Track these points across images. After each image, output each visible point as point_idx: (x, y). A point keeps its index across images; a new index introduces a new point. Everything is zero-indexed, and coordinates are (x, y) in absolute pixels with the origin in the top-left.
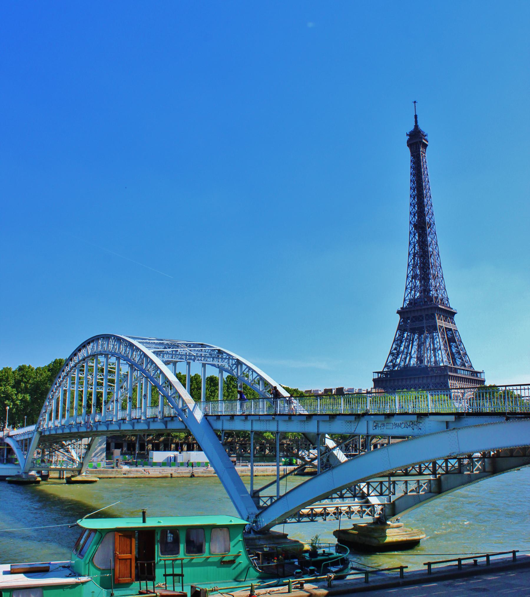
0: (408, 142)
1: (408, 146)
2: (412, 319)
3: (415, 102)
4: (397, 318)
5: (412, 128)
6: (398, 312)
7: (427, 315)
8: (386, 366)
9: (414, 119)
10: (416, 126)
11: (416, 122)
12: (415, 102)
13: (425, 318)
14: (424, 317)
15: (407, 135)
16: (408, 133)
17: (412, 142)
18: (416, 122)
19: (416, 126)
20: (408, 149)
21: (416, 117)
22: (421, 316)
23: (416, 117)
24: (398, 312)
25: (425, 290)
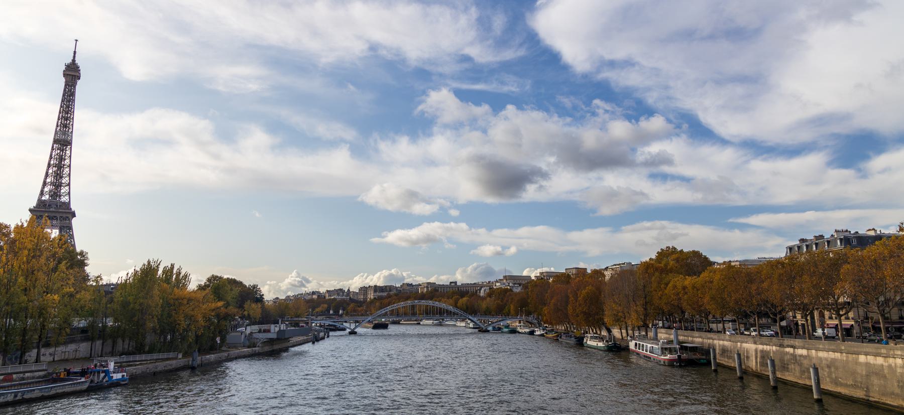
0: (64, 71)
5: (69, 61)
6: (30, 210)
7: (62, 217)
9: (73, 55)
10: (74, 60)
11: (74, 57)
12: (76, 40)
13: (60, 219)
14: (59, 219)
15: (66, 65)
16: (67, 64)
17: (68, 73)
18: (74, 57)
19: (74, 60)
20: (63, 80)
21: (75, 52)
22: (55, 217)
23: (75, 52)
24: (30, 210)
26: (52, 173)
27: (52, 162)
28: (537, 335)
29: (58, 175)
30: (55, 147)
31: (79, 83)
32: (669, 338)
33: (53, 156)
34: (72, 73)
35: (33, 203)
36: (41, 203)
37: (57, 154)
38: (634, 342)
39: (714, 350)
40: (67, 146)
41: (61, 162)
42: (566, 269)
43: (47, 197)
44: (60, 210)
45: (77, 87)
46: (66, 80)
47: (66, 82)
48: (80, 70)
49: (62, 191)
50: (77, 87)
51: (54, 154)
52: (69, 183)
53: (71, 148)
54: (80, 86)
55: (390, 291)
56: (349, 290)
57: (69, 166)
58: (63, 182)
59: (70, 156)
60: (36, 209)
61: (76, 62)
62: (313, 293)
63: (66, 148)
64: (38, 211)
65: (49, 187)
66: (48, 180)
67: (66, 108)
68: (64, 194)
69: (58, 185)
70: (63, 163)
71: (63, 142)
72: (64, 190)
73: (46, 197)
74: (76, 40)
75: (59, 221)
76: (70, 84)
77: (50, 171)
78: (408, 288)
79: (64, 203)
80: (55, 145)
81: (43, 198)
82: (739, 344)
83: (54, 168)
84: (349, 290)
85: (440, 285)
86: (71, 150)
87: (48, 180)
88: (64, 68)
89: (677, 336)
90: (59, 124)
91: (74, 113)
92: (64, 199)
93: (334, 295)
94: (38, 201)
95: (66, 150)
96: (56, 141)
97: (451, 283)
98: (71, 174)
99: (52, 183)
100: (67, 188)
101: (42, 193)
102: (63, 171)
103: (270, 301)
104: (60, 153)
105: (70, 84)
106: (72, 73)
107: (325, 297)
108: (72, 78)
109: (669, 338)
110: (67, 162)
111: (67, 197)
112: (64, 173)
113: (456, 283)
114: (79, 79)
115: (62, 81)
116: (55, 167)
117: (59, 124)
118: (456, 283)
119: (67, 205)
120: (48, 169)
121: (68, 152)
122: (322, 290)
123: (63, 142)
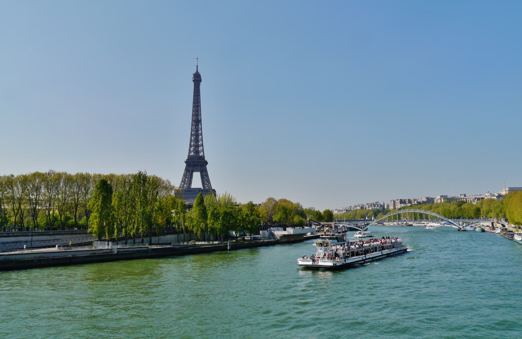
2: (193, 166)
3: (197, 59)
4: (185, 164)
5: (195, 72)
8: (181, 187)
9: (196, 67)
10: (197, 71)
15: (193, 75)
17: (195, 79)
19: (197, 71)
20: (193, 83)
21: (197, 66)
22: (197, 165)
23: (197, 66)
25: (197, 152)
29: (197, 140)
31: (201, 84)
34: (197, 79)
35: (186, 158)
40: (199, 122)
41: (197, 132)
44: (200, 161)
45: (200, 86)
46: (194, 83)
47: (194, 84)
48: (201, 76)
49: (200, 149)
50: (201, 87)
51: (193, 128)
57: (201, 134)
60: (188, 161)
61: (199, 72)
64: (189, 162)
65: (193, 147)
69: (197, 146)
70: (198, 133)
71: (197, 121)
72: (200, 149)
73: (192, 154)
74: (197, 59)
75: (199, 167)
76: (197, 85)
77: (192, 138)
79: (201, 156)
81: (191, 154)
87: (192, 144)
88: (192, 76)
90: (194, 110)
92: (201, 154)
95: (199, 125)
96: (193, 121)
99: (194, 146)
100: (201, 147)
105: (197, 85)
106: (197, 79)
108: (197, 82)
111: (202, 153)
112: (199, 139)
117: (194, 110)
119: (203, 158)
120: (191, 138)
121: (200, 126)
123: (197, 121)
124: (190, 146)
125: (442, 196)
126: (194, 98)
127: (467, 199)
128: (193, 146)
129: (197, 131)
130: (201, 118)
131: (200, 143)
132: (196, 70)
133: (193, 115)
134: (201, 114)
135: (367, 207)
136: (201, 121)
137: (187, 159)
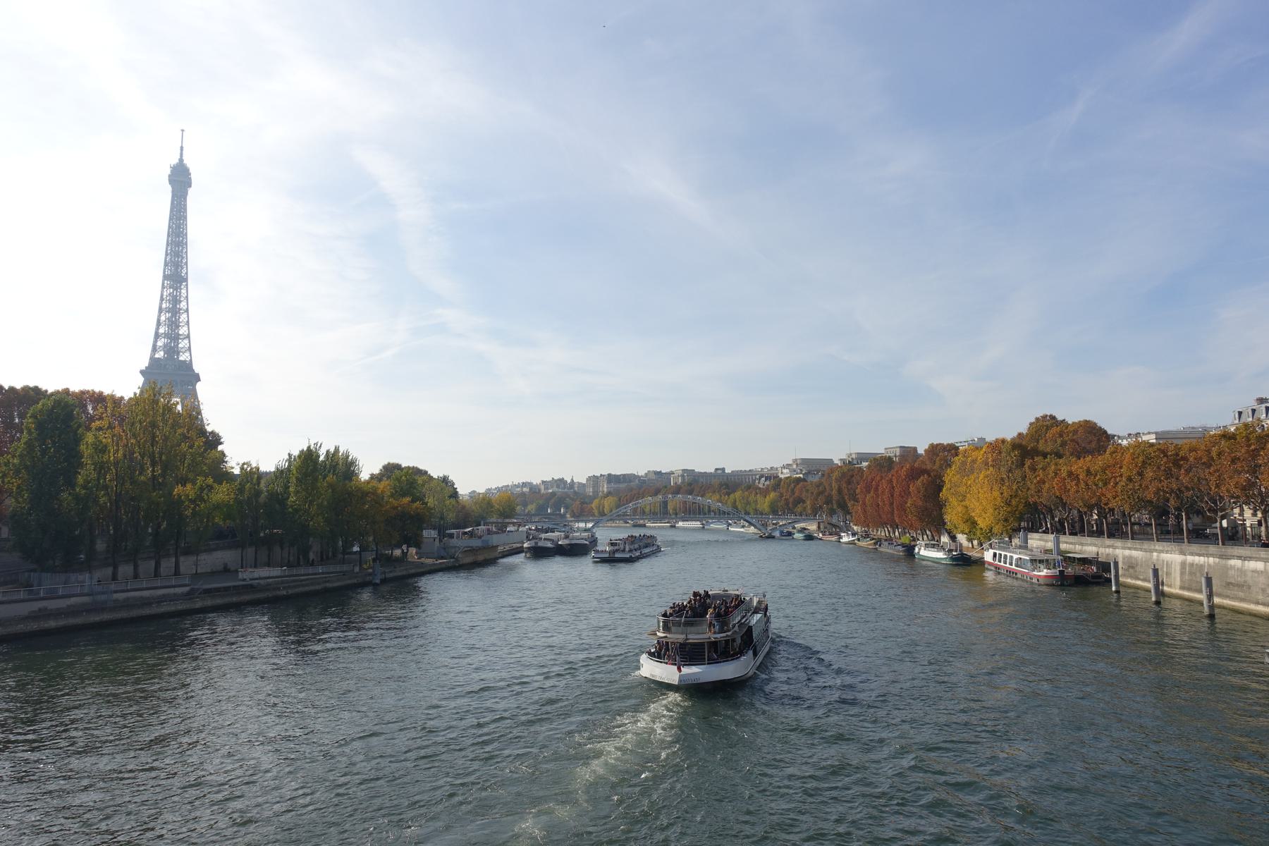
0: (169, 176)
1: (169, 180)
5: (175, 161)
9: (179, 151)
10: (181, 160)
11: (181, 155)
12: (183, 131)
18: (181, 155)
19: (181, 160)
20: (169, 188)
21: (182, 148)
23: (182, 148)
24: (142, 372)
25: (172, 351)
26: (165, 321)
27: (164, 306)
28: (843, 543)
29: (174, 324)
30: (165, 285)
31: (191, 191)
32: (1045, 546)
33: (165, 297)
34: (180, 178)
35: (144, 363)
36: (153, 361)
37: (170, 294)
38: (991, 552)
39: (1116, 564)
41: (176, 306)
42: (886, 449)
43: (162, 353)
47: (173, 192)
48: (190, 174)
49: (180, 345)
51: (165, 294)
52: (189, 334)
53: (187, 285)
54: (192, 194)
55: (630, 481)
56: (572, 480)
57: (187, 311)
58: (180, 333)
59: (187, 297)
61: (185, 162)
62: (524, 484)
63: (181, 286)
65: (163, 340)
66: (161, 331)
67: (176, 229)
68: (183, 350)
69: (174, 337)
70: (178, 306)
71: (175, 276)
73: (160, 354)
74: (183, 131)
78: (654, 477)
80: (166, 282)
82: (1155, 554)
83: (167, 314)
84: (572, 480)
85: (701, 473)
86: (187, 288)
87: (161, 331)
88: (168, 171)
89: (1057, 543)
90: (169, 252)
91: (186, 236)
93: (552, 487)
94: (150, 359)
95: (181, 289)
96: (165, 277)
97: (717, 469)
98: (190, 323)
99: (166, 335)
101: (154, 349)
102: (179, 318)
103: (465, 495)
104: (173, 292)
106: (180, 178)
107: (540, 490)
109: (1045, 546)
110: (183, 305)
112: (181, 320)
113: (723, 469)
114: (190, 186)
115: (168, 189)
116: (169, 312)
117: (169, 252)
118: (723, 469)
119: (188, 366)
120: (159, 316)
121: (184, 291)
122: (536, 481)
123: (175, 276)
124: (157, 336)
125: (684, 470)
126: (169, 224)
127: (747, 477)
128: (164, 338)
129: (175, 300)
130: (187, 273)
131: (183, 331)
132: (179, 155)
133: (166, 264)
134: (186, 263)
135: (542, 487)
136: (186, 280)
137: (147, 365)
